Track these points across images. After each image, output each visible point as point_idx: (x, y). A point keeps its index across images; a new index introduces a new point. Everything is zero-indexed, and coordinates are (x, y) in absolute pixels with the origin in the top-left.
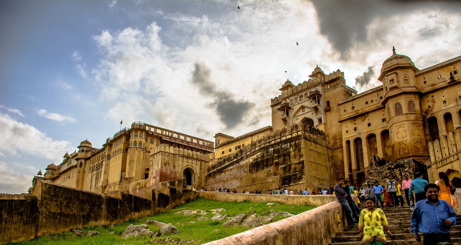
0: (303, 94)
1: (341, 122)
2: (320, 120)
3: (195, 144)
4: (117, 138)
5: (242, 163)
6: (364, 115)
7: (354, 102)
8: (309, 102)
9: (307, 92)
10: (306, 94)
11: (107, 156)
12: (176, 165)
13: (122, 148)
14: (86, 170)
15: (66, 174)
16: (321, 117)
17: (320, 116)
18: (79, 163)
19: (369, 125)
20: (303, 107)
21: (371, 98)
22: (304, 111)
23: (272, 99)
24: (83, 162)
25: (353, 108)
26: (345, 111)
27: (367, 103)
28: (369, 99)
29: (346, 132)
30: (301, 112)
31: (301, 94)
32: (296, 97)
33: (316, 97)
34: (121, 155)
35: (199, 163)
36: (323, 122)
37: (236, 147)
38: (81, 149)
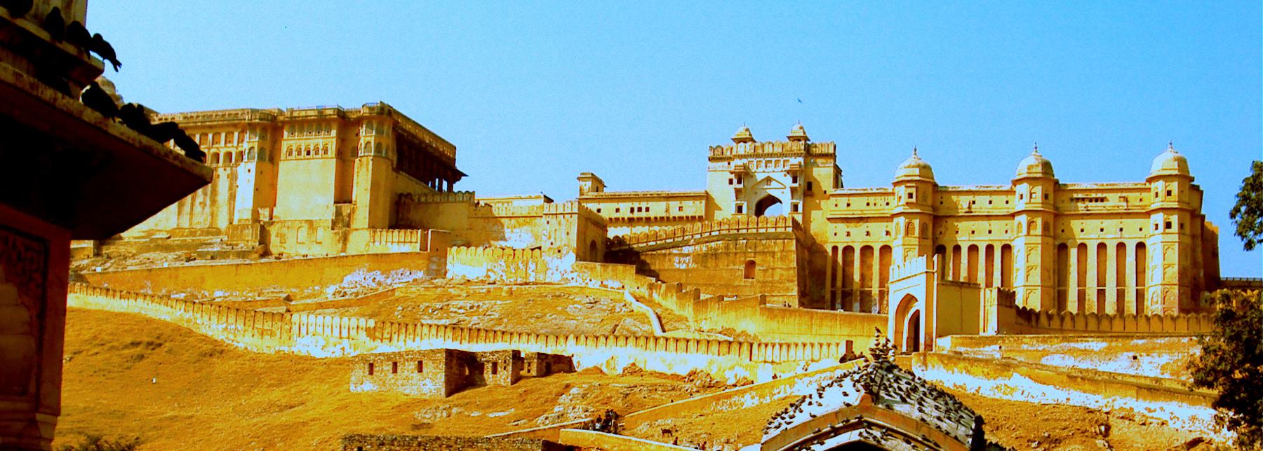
5: (686, 250)
10: (777, 162)
19: (868, 234)
28: (872, 200)
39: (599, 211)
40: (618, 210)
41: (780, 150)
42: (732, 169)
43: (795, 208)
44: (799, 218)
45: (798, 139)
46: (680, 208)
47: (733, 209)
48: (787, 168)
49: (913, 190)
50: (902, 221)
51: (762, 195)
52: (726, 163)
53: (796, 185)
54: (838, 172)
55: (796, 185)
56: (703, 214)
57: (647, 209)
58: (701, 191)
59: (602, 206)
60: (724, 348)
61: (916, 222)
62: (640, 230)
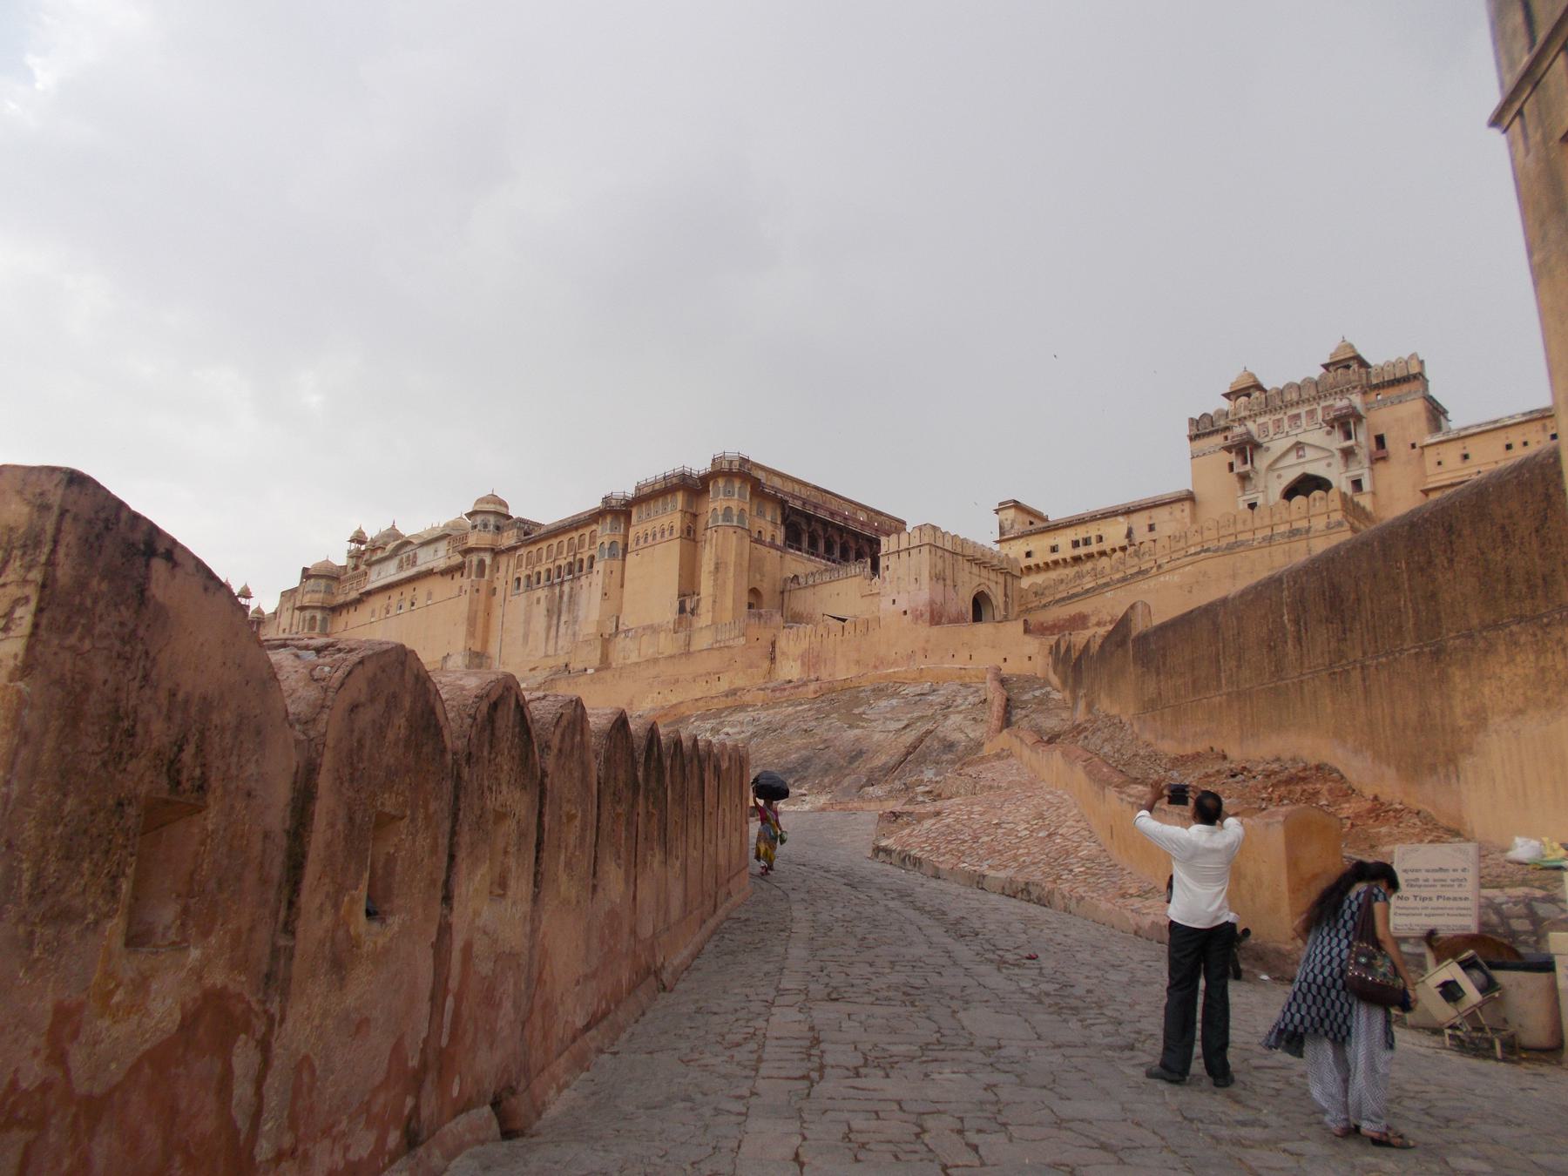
0: (1303, 410)
2: (1357, 484)
3: (862, 524)
4: (650, 496)
7: (1468, 442)
8: (1322, 433)
10: (1311, 413)
11: (607, 546)
12: (959, 583)
13: (677, 524)
14: (499, 585)
15: (395, 594)
18: (475, 562)
20: (1299, 447)
23: (1192, 420)
24: (488, 561)
30: (1292, 459)
31: (1295, 411)
33: (1345, 423)
34: (674, 548)
35: (1001, 579)
36: (1366, 485)
38: (479, 519)
41: (1313, 393)
51: (1290, 476)
57: (1100, 539)
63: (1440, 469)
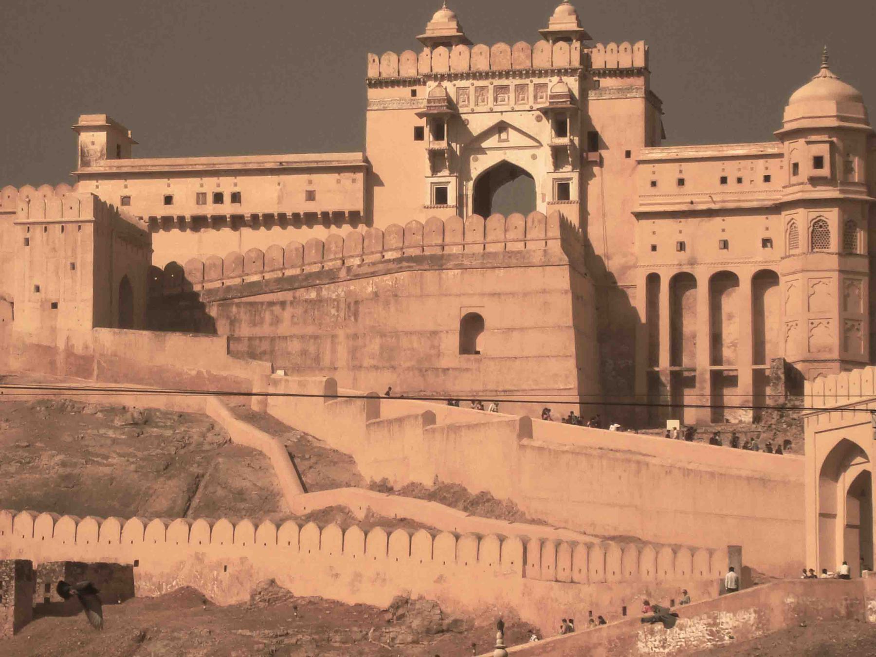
0: (512, 82)
1: (640, 216)
5: (329, 292)
6: (710, 213)
9: (527, 81)
10: (521, 88)
16: (571, 179)
17: (568, 175)
21: (739, 170)
22: (507, 140)
25: (681, 182)
26: (654, 184)
27: (724, 180)
29: (650, 248)
32: (481, 83)
37: (198, 194)
39: (126, 201)
40: (168, 200)
42: (423, 106)
43: (563, 191)
44: (571, 213)
45: (565, 37)
46: (311, 196)
47: (428, 196)
48: (544, 103)
49: (823, 150)
50: (802, 217)
52: (405, 92)
53: (564, 141)
54: (652, 101)
55: (564, 141)
56: (359, 206)
57: (236, 198)
58: (355, 158)
59: (134, 188)
60: (468, 545)
61: (832, 217)
62: (220, 244)
63: (653, 191)
